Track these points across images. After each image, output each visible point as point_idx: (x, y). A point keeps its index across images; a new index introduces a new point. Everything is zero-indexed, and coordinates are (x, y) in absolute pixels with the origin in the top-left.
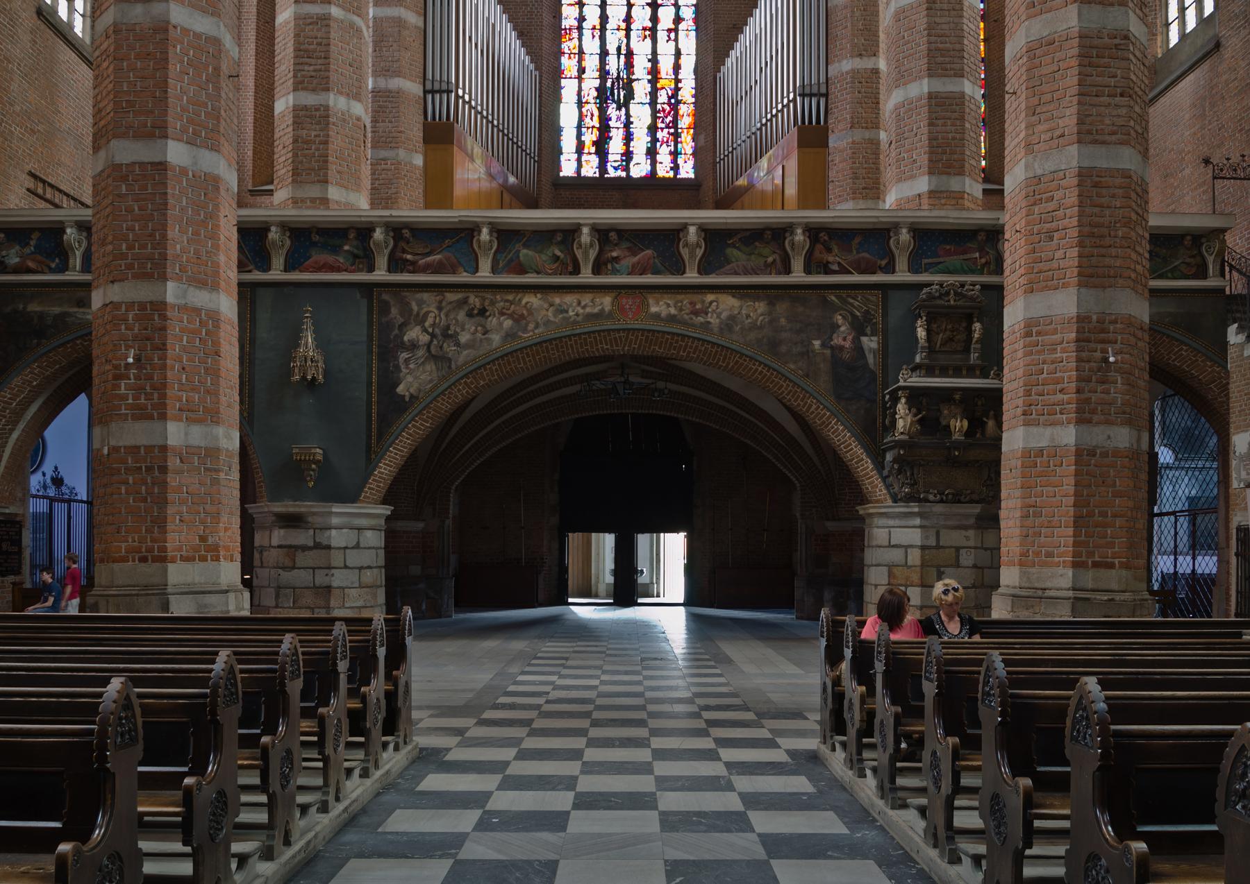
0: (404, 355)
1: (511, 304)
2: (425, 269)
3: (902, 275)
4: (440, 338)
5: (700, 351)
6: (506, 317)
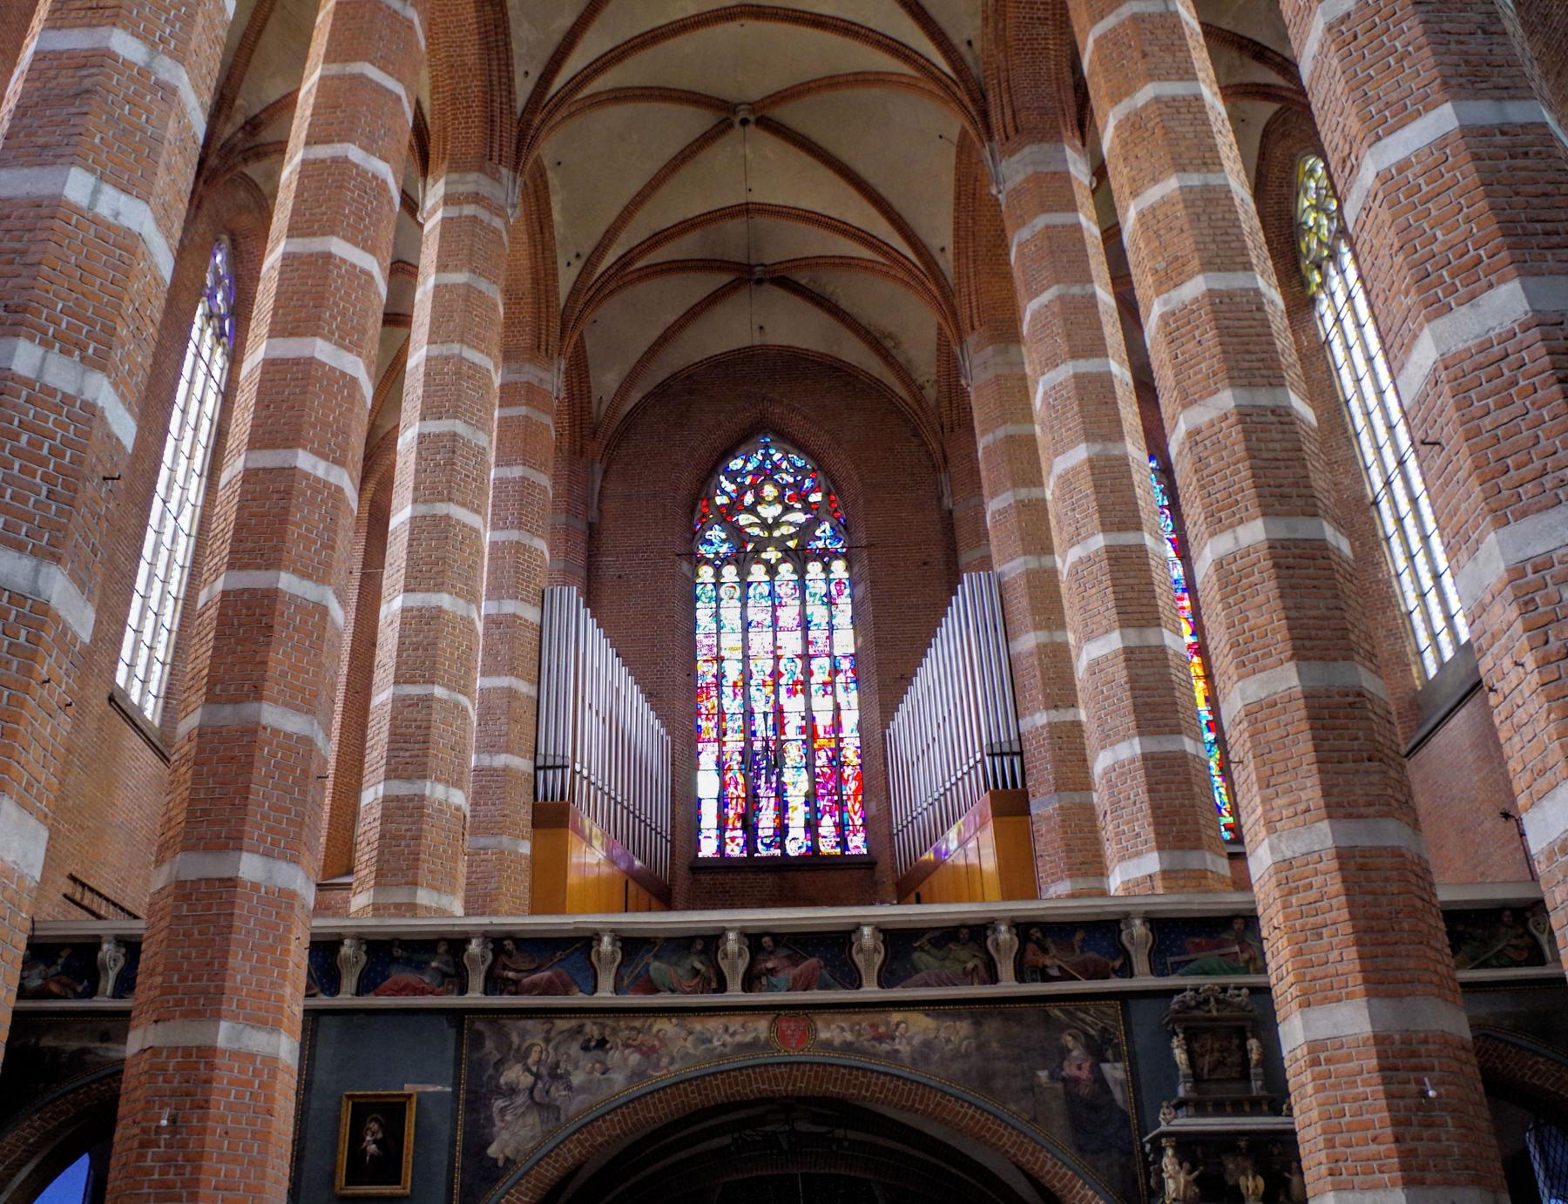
0: (499, 1103)
1: (639, 1033)
2: (530, 990)
3: (1143, 980)
4: (547, 1078)
5: (888, 1090)
6: (631, 1050)
